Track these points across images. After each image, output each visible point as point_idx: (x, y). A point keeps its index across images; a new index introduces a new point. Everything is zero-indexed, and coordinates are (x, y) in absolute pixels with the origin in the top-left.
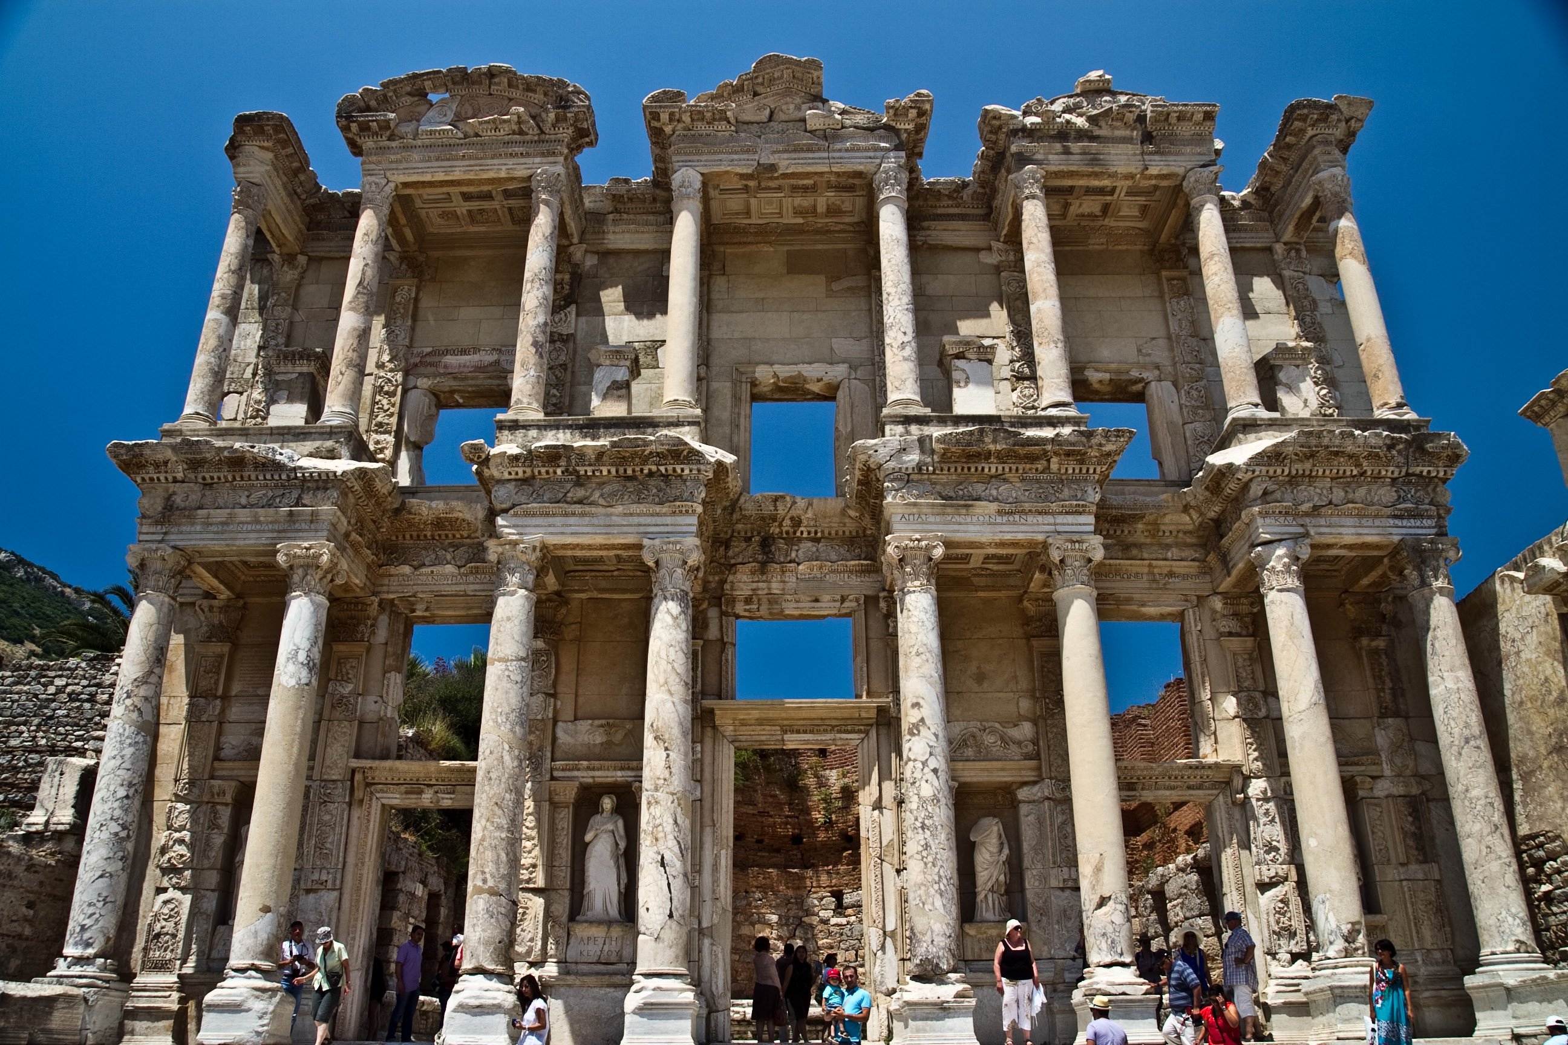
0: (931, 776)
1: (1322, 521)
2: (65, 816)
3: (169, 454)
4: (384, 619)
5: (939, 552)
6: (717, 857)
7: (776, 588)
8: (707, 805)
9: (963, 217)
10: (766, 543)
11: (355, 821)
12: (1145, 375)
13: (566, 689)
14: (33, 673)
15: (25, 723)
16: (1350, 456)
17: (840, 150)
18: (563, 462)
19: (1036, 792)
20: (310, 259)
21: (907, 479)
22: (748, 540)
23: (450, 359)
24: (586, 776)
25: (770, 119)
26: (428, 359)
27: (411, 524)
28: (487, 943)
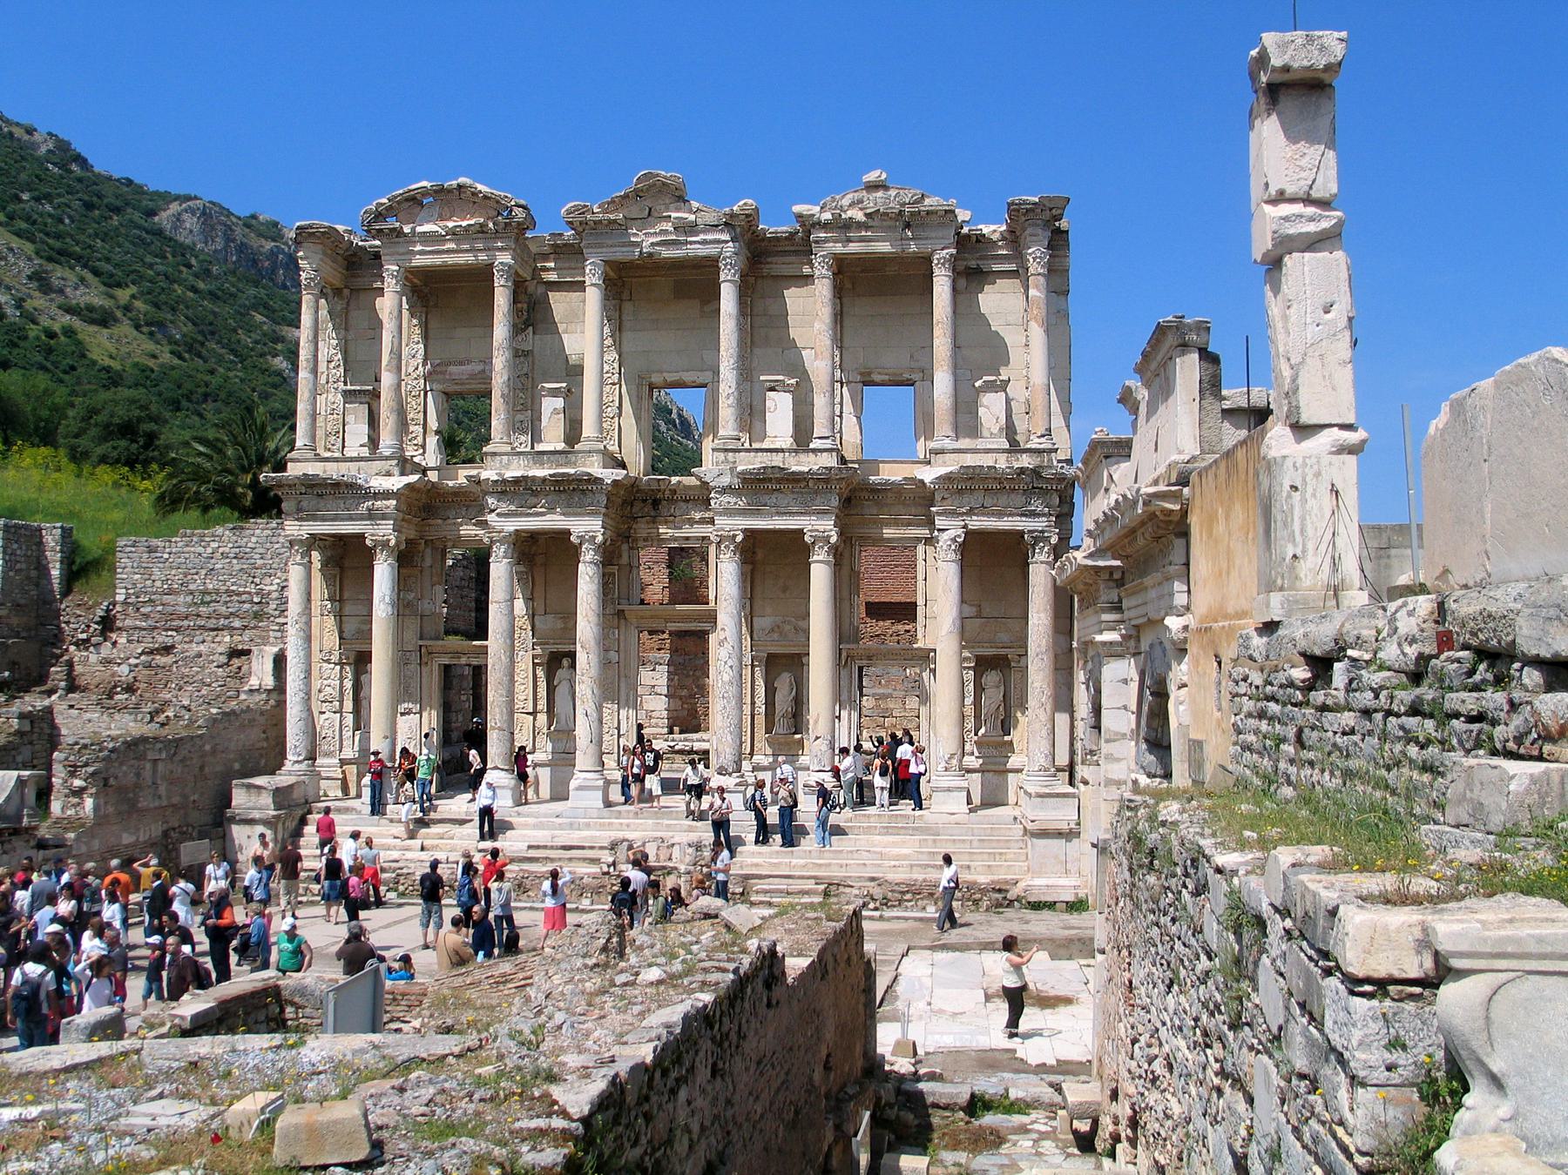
2: (269, 682)
4: (429, 551)
5: (739, 539)
10: (656, 503)
21: (724, 490)
23: (452, 369)
24: (554, 648)
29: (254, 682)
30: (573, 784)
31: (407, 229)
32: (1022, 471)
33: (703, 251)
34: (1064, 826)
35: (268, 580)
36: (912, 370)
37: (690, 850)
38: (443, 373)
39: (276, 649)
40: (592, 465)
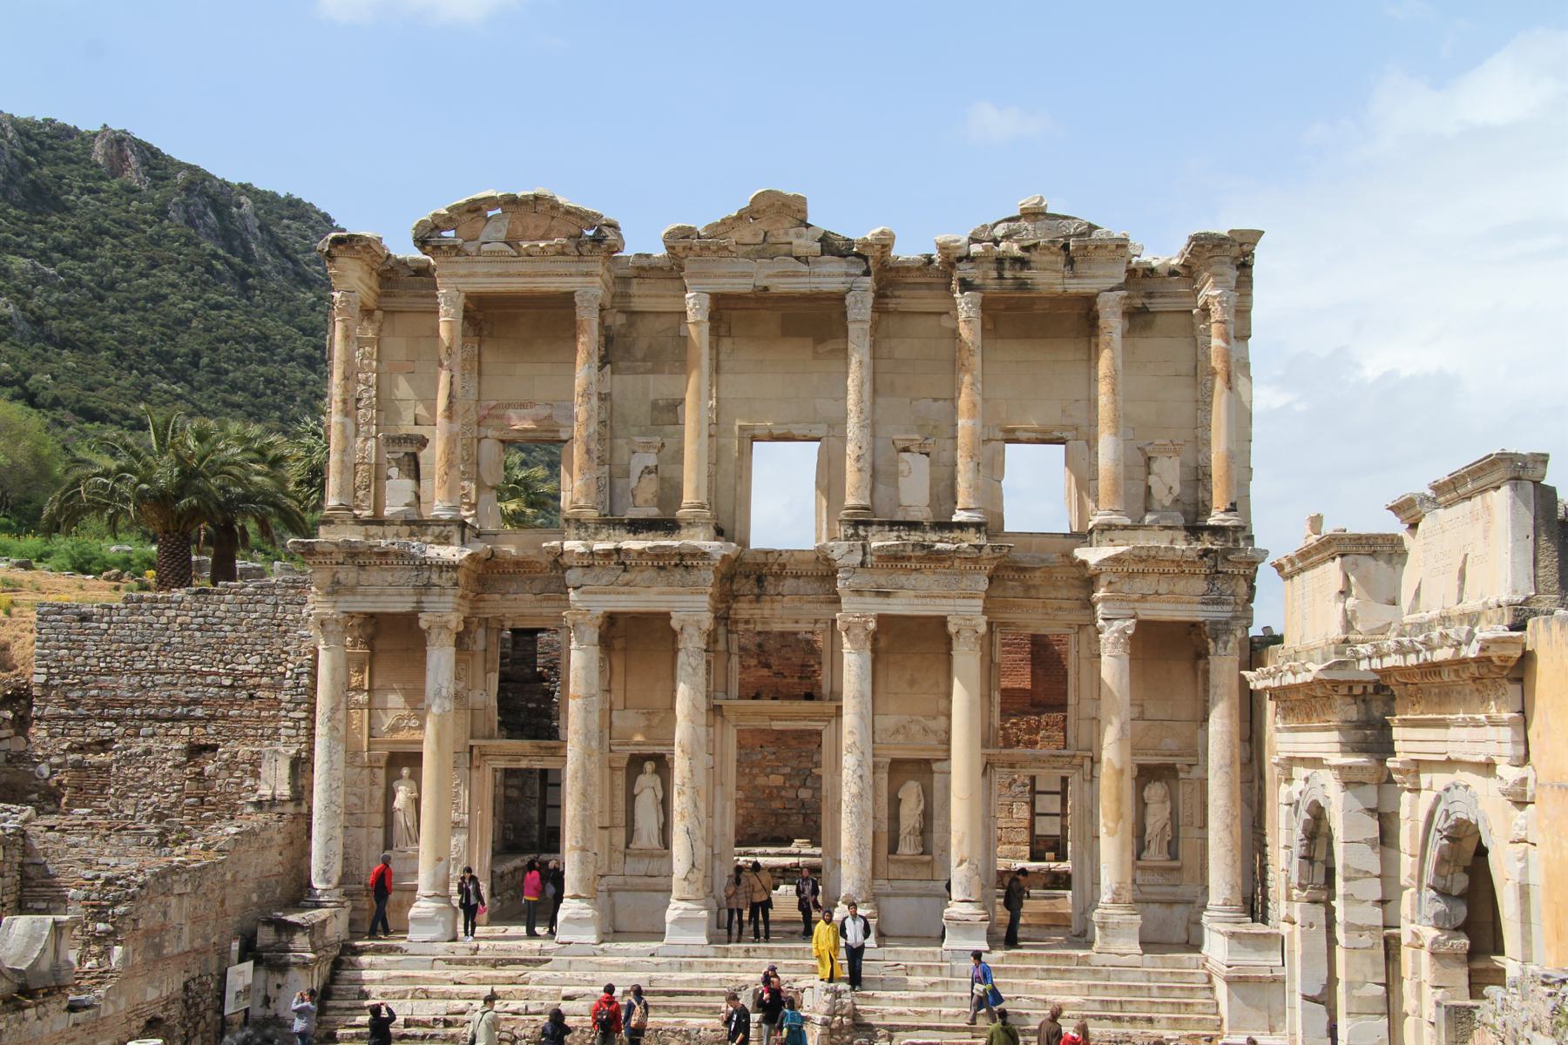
1: (1147, 605)
2: (284, 790)
3: (333, 548)
4: (481, 631)
5: (872, 625)
6: (724, 808)
7: (767, 612)
8: (717, 769)
9: (929, 286)
10: (760, 580)
11: (474, 780)
13: (617, 687)
14: (144, 605)
15: (146, 649)
18: (615, 557)
19: (944, 764)
22: (747, 577)
24: (635, 750)
27: (497, 564)
30: (671, 915)
31: (471, 247)
33: (832, 285)
35: (242, 659)
36: (1063, 427)
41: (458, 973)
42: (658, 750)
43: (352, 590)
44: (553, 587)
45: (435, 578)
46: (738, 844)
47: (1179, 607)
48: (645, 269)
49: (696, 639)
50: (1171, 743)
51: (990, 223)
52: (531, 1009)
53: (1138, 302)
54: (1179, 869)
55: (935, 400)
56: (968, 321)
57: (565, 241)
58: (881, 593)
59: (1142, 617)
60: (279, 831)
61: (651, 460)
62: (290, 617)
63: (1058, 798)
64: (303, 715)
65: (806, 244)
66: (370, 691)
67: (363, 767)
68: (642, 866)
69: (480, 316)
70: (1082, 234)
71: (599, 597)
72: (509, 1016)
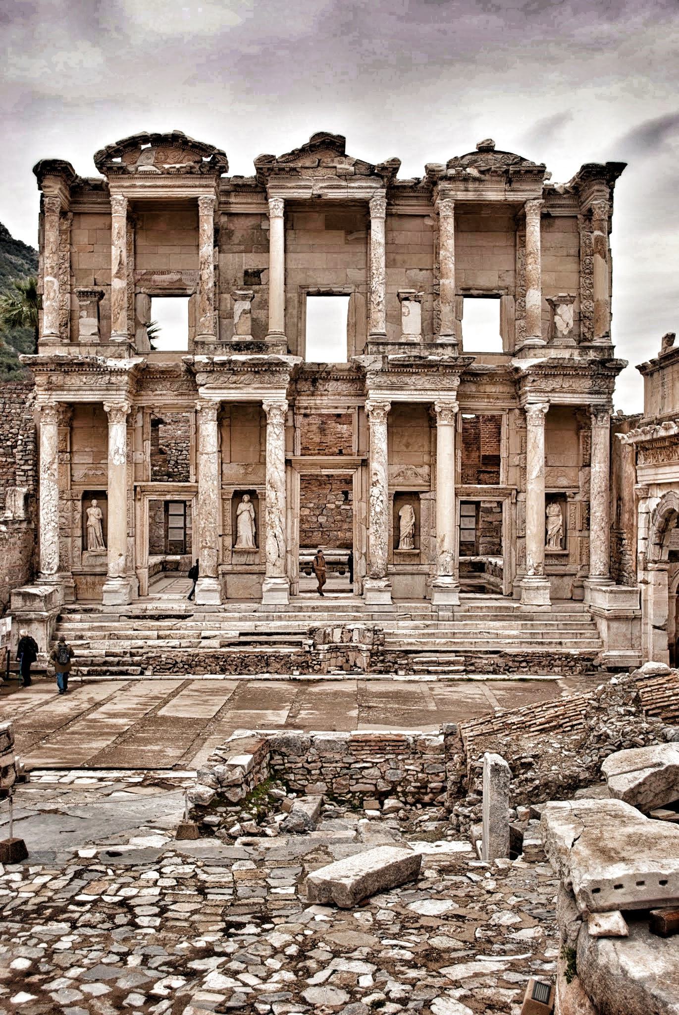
0: (380, 503)
1: (556, 395)
2: (21, 514)
4: (140, 415)
5: (388, 408)
6: (293, 523)
8: (289, 500)
10: (314, 382)
11: (138, 508)
12: (501, 292)
16: (572, 367)
17: (353, 188)
19: (427, 496)
20: (75, 214)
21: (376, 373)
24: (237, 488)
25: (319, 165)
26: (145, 277)
28: (209, 567)
29: (9, 514)
30: (265, 588)
31: (131, 168)
32: (593, 362)
33: (360, 194)
34: (630, 614)
36: (500, 288)
37: (369, 634)
38: (149, 280)
39: (25, 490)
40: (278, 352)
41: (137, 623)
42: (251, 487)
43: (61, 388)
44: (184, 387)
45: (113, 379)
46: (302, 546)
47: (575, 396)
48: (240, 187)
49: (278, 417)
50: (563, 482)
51: (459, 155)
52: (183, 645)
53: (545, 210)
54: (567, 555)
55: (421, 270)
56: (446, 217)
57: (192, 164)
58: (392, 387)
59: (552, 402)
60: (19, 539)
61: (247, 305)
62: (13, 411)
63: (474, 519)
64: (30, 467)
65: (345, 166)
66: (71, 452)
67: (68, 500)
68: (243, 559)
69: (135, 216)
70: (516, 163)
71: (218, 391)
72: (170, 649)
